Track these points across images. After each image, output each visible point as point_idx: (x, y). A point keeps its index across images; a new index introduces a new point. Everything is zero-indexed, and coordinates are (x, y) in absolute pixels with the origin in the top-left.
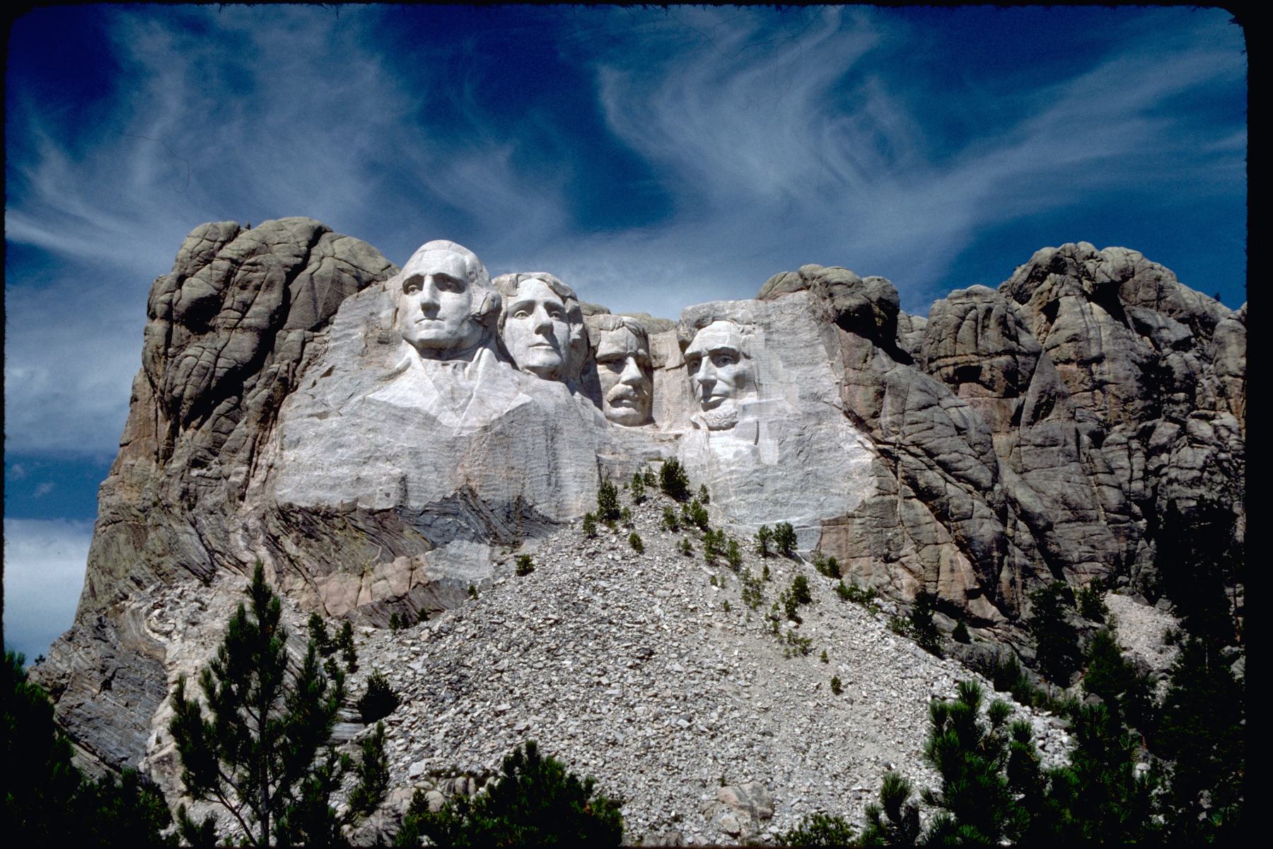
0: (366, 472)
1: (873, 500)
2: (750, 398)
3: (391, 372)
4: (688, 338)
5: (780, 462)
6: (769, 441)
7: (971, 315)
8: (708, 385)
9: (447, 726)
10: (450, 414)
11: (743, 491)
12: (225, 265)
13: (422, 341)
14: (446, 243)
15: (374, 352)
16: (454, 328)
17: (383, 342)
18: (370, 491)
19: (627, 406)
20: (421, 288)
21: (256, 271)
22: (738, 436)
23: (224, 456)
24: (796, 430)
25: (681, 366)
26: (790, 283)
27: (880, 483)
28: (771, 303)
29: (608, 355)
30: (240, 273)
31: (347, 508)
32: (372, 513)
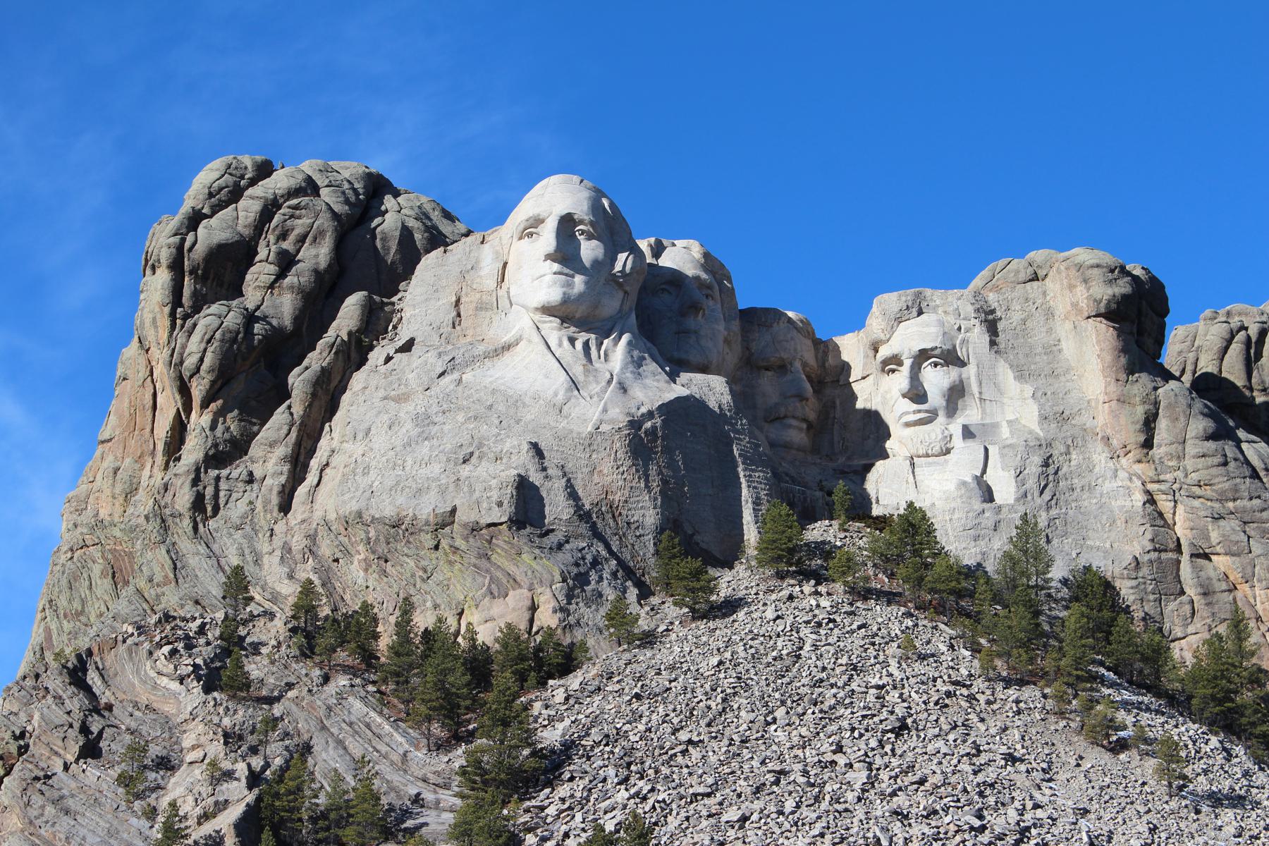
1: (1147, 557)
5: (1017, 500)
6: (1001, 473)
7: (1241, 336)
9: (619, 816)
12: (256, 206)
14: (576, 179)
19: (790, 426)
21: (299, 217)
23: (255, 450)
24: (1037, 460)
26: (1017, 272)
27: (1156, 535)
30: (277, 219)
31: (440, 520)
32: (475, 529)
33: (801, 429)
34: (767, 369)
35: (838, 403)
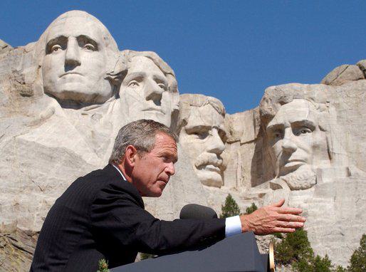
0: (23, 199)
2: (324, 164)
3: (35, 118)
4: (273, 113)
5: (357, 216)
6: (347, 199)
8: (288, 152)
10: (92, 154)
11: (328, 239)
13: (65, 92)
14: (84, 13)
15: (17, 103)
16: (92, 83)
17: (27, 95)
18: (27, 214)
19: (211, 170)
20: (64, 47)
22: (321, 193)
25: (255, 141)
26: (352, 73)
28: (339, 88)
29: (197, 127)
33: (217, 172)
34: (196, 133)
35: (239, 154)
